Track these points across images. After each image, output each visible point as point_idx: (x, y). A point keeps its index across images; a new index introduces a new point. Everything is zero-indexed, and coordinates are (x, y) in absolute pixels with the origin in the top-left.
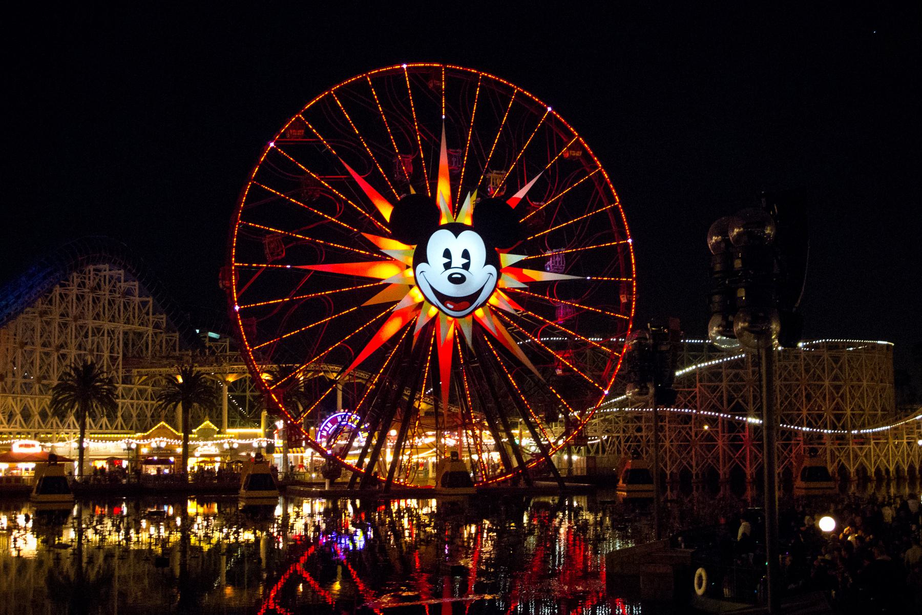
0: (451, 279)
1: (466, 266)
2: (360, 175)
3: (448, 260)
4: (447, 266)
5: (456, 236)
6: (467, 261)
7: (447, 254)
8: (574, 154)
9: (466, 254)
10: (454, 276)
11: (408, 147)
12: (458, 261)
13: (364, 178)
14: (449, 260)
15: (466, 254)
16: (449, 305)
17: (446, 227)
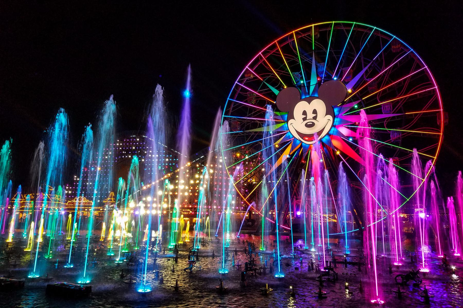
0: (307, 125)
1: (315, 118)
2: (273, 86)
3: (305, 116)
4: (305, 119)
5: (309, 104)
6: (316, 115)
7: (305, 113)
8: (395, 48)
9: (315, 112)
10: (308, 124)
11: (295, 68)
12: (310, 115)
13: (275, 88)
14: (305, 116)
15: (315, 112)
16: (307, 139)
17: (305, 100)
